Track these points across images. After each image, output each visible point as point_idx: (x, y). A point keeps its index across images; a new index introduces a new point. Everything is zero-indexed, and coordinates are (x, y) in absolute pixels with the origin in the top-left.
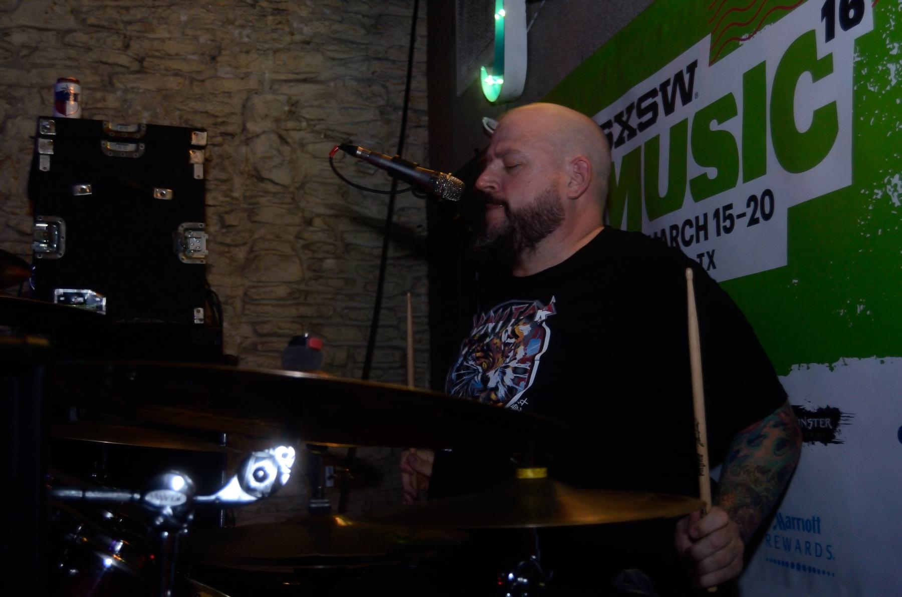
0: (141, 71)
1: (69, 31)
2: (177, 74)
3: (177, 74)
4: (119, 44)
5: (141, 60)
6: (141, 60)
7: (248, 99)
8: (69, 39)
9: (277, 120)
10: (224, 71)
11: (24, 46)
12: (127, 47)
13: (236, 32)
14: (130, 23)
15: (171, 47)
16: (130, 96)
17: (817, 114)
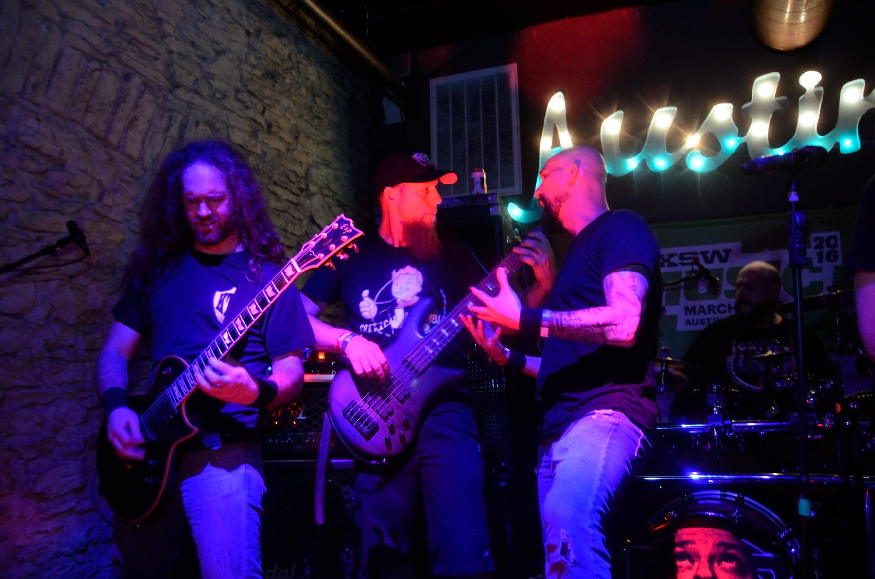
2: (282, 139)
3: (282, 139)
4: (262, 109)
5: (270, 126)
6: (270, 126)
7: (308, 169)
8: (240, 96)
9: (320, 188)
12: (263, 113)
13: (304, 124)
14: (265, 97)
15: (283, 123)
16: (266, 149)
17: (812, 283)
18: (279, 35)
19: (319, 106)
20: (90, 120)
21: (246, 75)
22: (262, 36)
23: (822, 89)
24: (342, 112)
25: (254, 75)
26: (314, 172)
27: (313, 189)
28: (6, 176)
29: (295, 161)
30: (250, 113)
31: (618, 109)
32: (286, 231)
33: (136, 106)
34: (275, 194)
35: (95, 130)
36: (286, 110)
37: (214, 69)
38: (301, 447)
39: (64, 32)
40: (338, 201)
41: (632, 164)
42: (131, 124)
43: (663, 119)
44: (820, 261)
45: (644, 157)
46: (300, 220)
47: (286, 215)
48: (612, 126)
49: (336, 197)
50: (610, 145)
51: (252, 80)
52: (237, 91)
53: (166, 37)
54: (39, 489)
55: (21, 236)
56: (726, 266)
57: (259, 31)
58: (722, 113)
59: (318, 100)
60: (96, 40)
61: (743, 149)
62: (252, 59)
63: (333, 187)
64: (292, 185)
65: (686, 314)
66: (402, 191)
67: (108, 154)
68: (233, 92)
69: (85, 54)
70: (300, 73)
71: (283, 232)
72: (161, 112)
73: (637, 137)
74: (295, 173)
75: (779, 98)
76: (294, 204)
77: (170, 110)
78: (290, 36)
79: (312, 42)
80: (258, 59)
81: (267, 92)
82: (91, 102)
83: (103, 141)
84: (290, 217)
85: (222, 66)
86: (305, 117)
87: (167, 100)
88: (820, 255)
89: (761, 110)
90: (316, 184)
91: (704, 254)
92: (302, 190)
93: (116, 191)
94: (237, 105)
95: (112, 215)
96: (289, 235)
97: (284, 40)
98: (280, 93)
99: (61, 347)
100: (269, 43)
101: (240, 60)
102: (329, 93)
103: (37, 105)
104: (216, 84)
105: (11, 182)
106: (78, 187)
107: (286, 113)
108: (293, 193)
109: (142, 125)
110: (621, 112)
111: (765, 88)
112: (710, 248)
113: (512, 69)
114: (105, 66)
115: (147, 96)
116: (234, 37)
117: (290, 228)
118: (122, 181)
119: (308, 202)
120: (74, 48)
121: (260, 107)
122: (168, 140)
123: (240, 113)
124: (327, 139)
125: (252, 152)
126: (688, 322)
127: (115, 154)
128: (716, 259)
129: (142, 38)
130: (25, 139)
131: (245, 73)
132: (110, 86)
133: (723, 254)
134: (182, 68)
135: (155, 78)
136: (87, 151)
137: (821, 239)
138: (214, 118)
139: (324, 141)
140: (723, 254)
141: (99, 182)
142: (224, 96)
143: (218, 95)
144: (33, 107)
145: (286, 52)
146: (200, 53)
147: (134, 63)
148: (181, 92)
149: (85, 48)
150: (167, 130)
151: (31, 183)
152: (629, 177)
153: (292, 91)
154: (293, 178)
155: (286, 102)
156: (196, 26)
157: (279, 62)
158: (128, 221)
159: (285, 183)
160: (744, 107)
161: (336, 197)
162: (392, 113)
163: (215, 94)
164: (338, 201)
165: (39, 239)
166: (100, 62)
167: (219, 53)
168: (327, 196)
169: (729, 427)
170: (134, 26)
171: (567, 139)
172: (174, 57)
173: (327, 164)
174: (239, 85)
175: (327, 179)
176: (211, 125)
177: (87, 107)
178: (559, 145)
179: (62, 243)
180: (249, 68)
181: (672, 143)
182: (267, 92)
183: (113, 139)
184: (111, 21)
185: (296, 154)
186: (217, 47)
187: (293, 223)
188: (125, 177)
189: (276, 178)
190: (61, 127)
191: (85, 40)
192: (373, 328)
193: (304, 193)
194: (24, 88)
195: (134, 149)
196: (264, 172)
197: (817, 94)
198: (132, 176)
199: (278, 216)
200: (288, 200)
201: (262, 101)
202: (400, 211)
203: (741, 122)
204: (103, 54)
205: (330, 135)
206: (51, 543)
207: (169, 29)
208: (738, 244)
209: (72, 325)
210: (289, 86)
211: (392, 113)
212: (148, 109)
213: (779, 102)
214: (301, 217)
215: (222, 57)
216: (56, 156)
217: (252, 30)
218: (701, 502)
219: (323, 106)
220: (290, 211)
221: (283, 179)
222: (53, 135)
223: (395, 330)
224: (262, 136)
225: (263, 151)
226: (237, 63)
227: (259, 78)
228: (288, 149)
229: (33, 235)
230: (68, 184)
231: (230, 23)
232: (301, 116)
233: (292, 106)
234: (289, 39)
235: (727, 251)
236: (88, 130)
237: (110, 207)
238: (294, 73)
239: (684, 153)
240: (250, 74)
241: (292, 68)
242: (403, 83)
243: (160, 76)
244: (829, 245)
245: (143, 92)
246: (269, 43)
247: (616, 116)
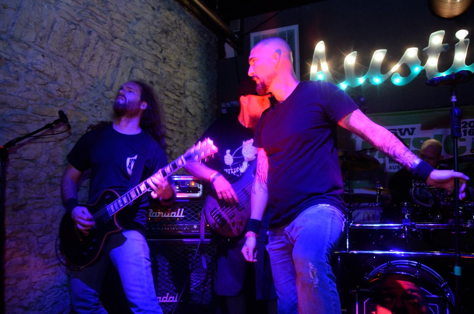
0: (164, 62)
1: (148, 40)
2: (171, 66)
3: (171, 66)
5: (165, 59)
6: (165, 59)
7: (185, 82)
9: (191, 92)
10: (180, 70)
11: (138, 40)
12: (161, 52)
13: (183, 58)
14: (162, 44)
15: (172, 57)
16: (163, 72)
18: (170, 10)
19: (191, 48)
20: (71, 56)
21: (152, 32)
22: (161, 10)
23: (468, 39)
24: (203, 51)
25: (156, 31)
26: (188, 84)
27: (187, 93)
28: (27, 86)
29: (178, 78)
30: (154, 52)
31: (354, 50)
32: (173, 116)
33: (94, 49)
34: (167, 96)
35: (72, 61)
36: (173, 50)
37: (136, 28)
38: (181, 232)
39: (57, 9)
40: (201, 99)
41: (361, 81)
42: (92, 58)
43: (379, 56)
44: (465, 135)
45: (368, 77)
46: (181, 110)
47: (173, 107)
48: (351, 60)
49: (199, 98)
50: (349, 70)
51: (155, 34)
52: (148, 40)
53: (110, 11)
54: (44, 252)
55: (35, 118)
56: (412, 137)
57: (159, 7)
58: (411, 53)
59: (191, 45)
60: (73, 14)
61: (423, 72)
62: (155, 23)
63: (198, 92)
64: (176, 91)
65: (389, 163)
66: (249, 99)
67: (80, 74)
68: (145, 41)
69: (68, 21)
70: (181, 30)
71: (171, 117)
72: (108, 52)
73: (364, 65)
74: (178, 84)
75: (444, 45)
76: (178, 101)
77: (112, 50)
78: (175, 10)
79: (187, 13)
80: (159, 22)
81: (163, 41)
82: (71, 47)
83: (77, 67)
84: (175, 109)
85: (139, 27)
86: (184, 55)
87: (110, 45)
88: (465, 131)
89: (433, 51)
90: (189, 90)
91: (400, 130)
92: (181, 94)
93: (84, 94)
94: (147, 48)
95: (82, 107)
96: (175, 118)
97: (172, 12)
98: (170, 41)
99: (55, 177)
100: (164, 14)
101: (149, 23)
102: (196, 41)
103: (43, 48)
104: (137, 36)
105: (29, 90)
106: (64, 92)
107: (173, 51)
108: (177, 96)
109: (97, 59)
110: (356, 52)
111: (436, 39)
112: (403, 127)
113: (295, 28)
114: (78, 27)
115: (100, 43)
116: (146, 11)
117: (175, 114)
118: (86, 89)
119: (185, 100)
120: (61, 17)
121: (159, 49)
122: (111, 67)
123: (149, 52)
124: (195, 66)
125: (155, 73)
126: (390, 167)
127: (84, 74)
128: (407, 133)
129: (98, 12)
130: (37, 67)
131: (152, 30)
132: (80, 38)
133: (411, 130)
134: (118, 28)
135: (105, 33)
136: (68, 73)
137: (466, 123)
138: (135, 55)
139: (193, 67)
140: (411, 130)
141: (75, 89)
142: (141, 43)
143: (138, 43)
144: (41, 49)
145: (173, 19)
146: (128, 19)
147: (93, 26)
148: (117, 41)
149: (68, 17)
150: (110, 62)
151: (40, 90)
152: (360, 87)
153: (177, 40)
154: (177, 87)
155: (173, 46)
156: (126, 5)
157: (170, 24)
158: (90, 110)
159: (172, 90)
160: (424, 49)
161: (199, 98)
162: (230, 52)
163: (136, 42)
164: (201, 99)
165: (44, 120)
166: (75, 24)
167: (138, 19)
168: (195, 97)
169: (414, 226)
170: (93, 6)
171: (325, 66)
172: (115, 22)
173: (195, 80)
174: (148, 37)
175: (195, 88)
176: (133, 59)
177: (68, 49)
178: (321, 70)
179: (56, 122)
180: (154, 28)
181: (384, 68)
182: (163, 41)
183: (82, 66)
184: (81, 3)
185: (178, 75)
186: (137, 16)
187: (177, 112)
188: (88, 86)
189: (168, 87)
190: (55, 60)
191: (68, 13)
192: (230, 171)
193: (183, 95)
194: (36, 39)
195: (94, 72)
196: (162, 84)
197: (466, 42)
198: (92, 86)
199: (169, 107)
200: (174, 99)
201: (160, 46)
202: (248, 110)
203: (423, 58)
204: (76, 20)
205: (196, 64)
206: (50, 280)
207: (111, 7)
208: (420, 125)
209: (60, 166)
210: (175, 38)
211: (230, 52)
212: (101, 50)
213: (443, 46)
214: (181, 108)
215: (140, 21)
216: (53, 75)
217: (155, 7)
218: (397, 266)
219: (193, 48)
220: (175, 105)
221: (172, 88)
222: (51, 63)
223: (242, 173)
224: (161, 64)
225: (161, 73)
226: (147, 25)
227: (159, 33)
228: (175, 72)
229: (41, 118)
230: (59, 90)
231: (144, 3)
232: (181, 54)
233: (176, 48)
234: (175, 12)
235: (413, 129)
236: (69, 61)
237: (81, 103)
238: (177, 30)
239: (390, 74)
240: (154, 31)
241: (176, 28)
242: (236, 36)
243: (107, 32)
244: (470, 126)
245: (98, 41)
246: (164, 14)
247: (353, 54)
